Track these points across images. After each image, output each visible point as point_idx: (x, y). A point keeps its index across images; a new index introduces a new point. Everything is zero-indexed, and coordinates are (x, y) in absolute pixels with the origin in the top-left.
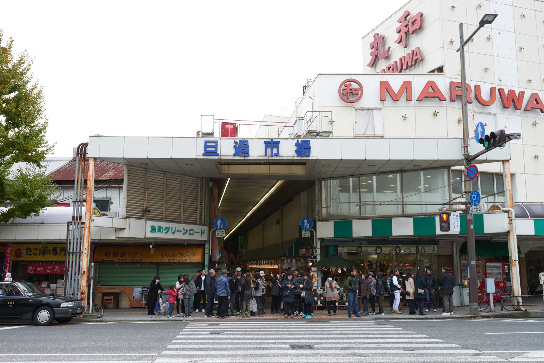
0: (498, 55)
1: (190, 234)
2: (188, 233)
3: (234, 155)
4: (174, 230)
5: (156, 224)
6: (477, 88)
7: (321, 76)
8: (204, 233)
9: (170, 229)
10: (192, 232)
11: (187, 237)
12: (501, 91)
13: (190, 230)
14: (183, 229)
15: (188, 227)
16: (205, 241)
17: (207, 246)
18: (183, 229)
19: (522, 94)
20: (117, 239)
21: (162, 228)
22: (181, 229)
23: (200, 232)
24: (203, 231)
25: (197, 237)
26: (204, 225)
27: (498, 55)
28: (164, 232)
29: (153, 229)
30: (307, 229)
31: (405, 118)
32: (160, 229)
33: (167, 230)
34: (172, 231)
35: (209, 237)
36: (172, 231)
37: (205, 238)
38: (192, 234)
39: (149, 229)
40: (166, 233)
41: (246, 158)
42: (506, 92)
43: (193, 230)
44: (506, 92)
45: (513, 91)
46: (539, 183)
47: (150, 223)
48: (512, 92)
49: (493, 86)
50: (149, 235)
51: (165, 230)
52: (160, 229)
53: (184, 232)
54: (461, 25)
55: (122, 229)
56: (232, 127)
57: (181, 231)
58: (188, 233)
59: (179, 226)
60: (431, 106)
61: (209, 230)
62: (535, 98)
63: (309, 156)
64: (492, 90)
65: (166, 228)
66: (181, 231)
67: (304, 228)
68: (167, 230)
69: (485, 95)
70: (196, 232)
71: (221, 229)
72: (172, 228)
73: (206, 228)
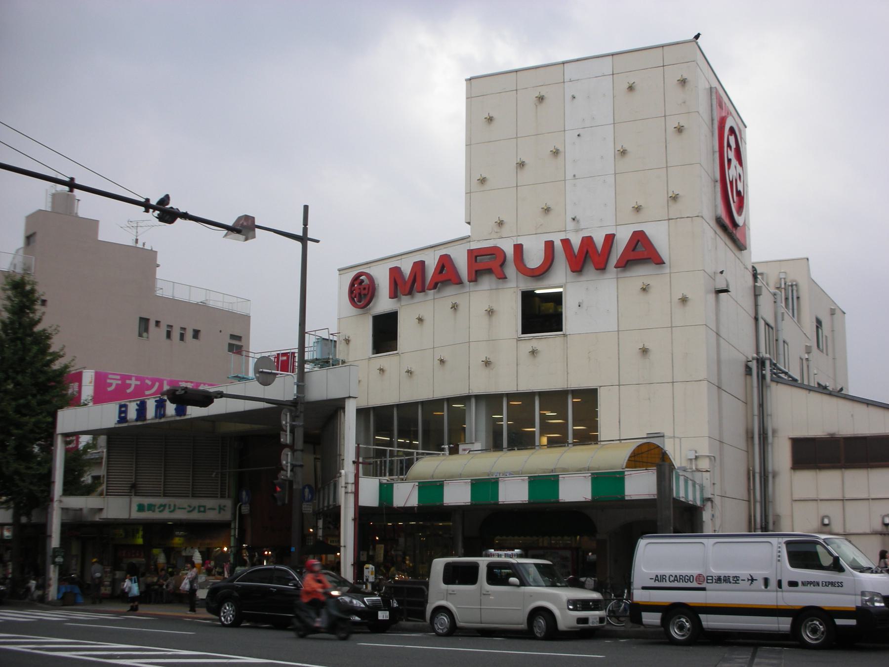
0: (574, 176)
1: (199, 511)
2: (196, 510)
3: (137, 420)
4: (172, 508)
5: (146, 501)
6: (518, 249)
7: (342, 272)
8: (224, 510)
9: (167, 507)
10: (202, 509)
11: (195, 516)
12: (566, 243)
13: (200, 507)
14: (190, 506)
15: (196, 502)
16: (231, 521)
17: (233, 526)
18: (190, 506)
19: (610, 239)
20: (101, 520)
21: (155, 506)
22: (186, 506)
23: (218, 508)
24: (222, 507)
25: (212, 516)
26: (229, 497)
27: (574, 176)
28: (157, 510)
29: (141, 508)
30: (308, 501)
31: (420, 320)
32: (151, 508)
33: (162, 508)
34: (170, 508)
35: (234, 514)
36: (170, 508)
37: (227, 516)
38: (204, 511)
39: (135, 508)
40: (160, 512)
41: (145, 423)
42: (576, 242)
43: (204, 507)
44: (576, 242)
45: (590, 239)
46: (649, 399)
47: (137, 500)
48: (588, 242)
49: (549, 238)
50: (136, 515)
51: (159, 508)
52: (151, 508)
53: (191, 509)
54: (306, 208)
55: (101, 510)
56: (285, 358)
57: (185, 509)
58: (196, 510)
59: (179, 501)
60: (450, 294)
61: (235, 505)
62: (639, 239)
63: (185, 414)
64: (549, 245)
65: (161, 506)
66: (185, 509)
67: (304, 499)
68: (162, 508)
69: (534, 258)
70: (209, 509)
71: (245, 503)
72: (170, 505)
73: (228, 503)
